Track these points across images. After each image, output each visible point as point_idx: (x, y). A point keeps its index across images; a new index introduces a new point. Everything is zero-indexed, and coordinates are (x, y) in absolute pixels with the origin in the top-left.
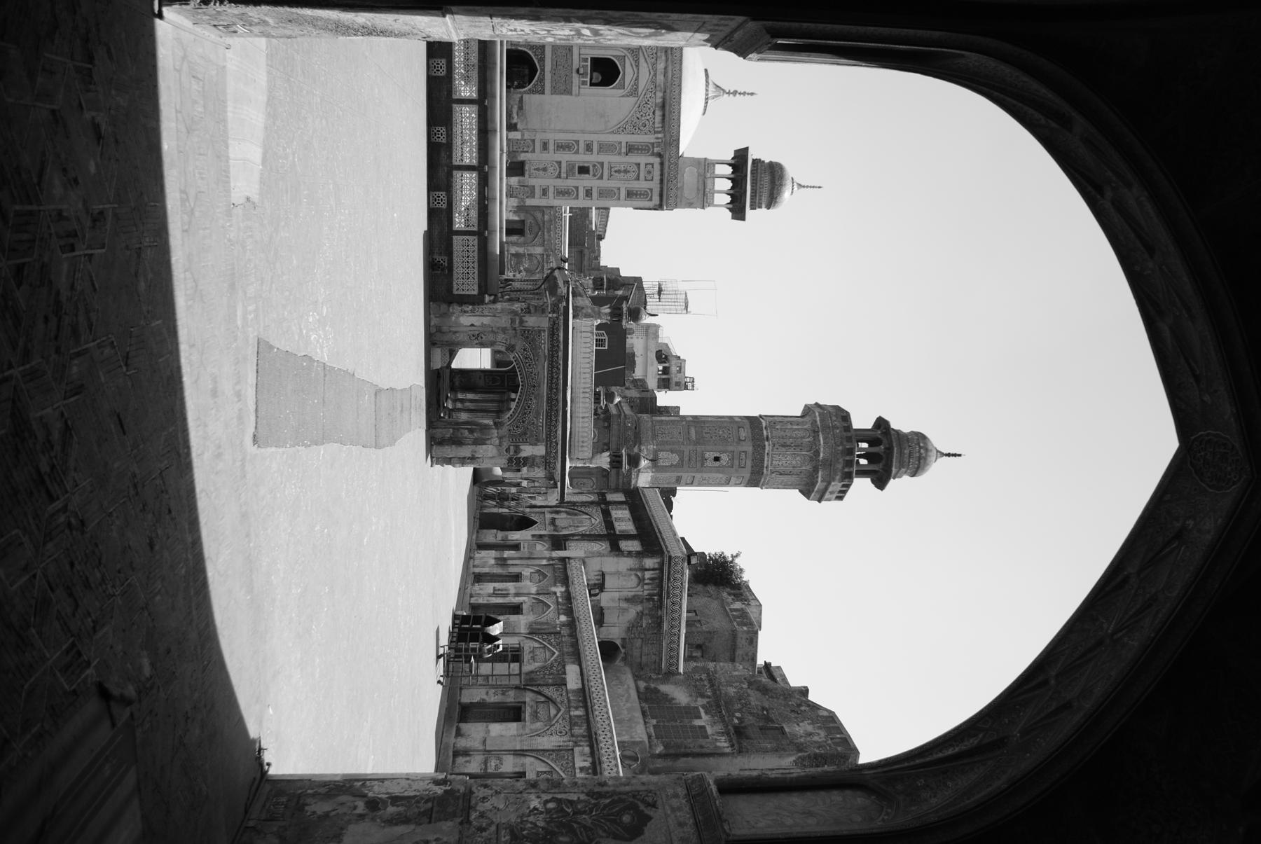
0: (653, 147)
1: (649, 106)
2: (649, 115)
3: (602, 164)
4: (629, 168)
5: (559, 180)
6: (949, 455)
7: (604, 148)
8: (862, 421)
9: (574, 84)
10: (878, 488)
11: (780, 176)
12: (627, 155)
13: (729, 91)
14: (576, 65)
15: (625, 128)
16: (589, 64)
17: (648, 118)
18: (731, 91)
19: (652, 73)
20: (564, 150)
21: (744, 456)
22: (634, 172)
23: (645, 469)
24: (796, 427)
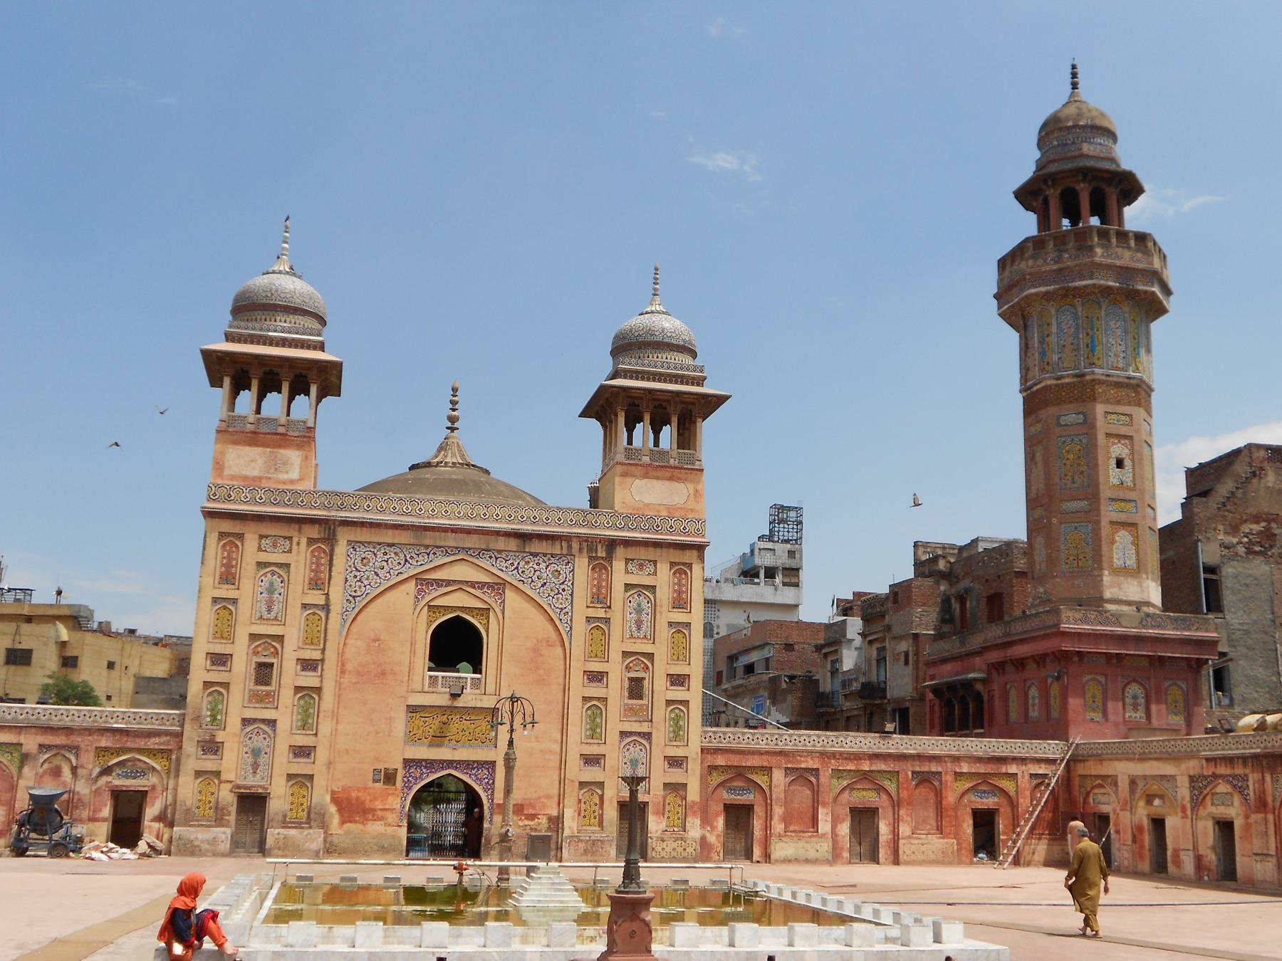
0: (597, 558)
1: (522, 563)
4: (634, 604)
8: (1026, 224)
9: (479, 705)
10: (1135, 199)
12: (610, 607)
13: (448, 428)
14: (442, 700)
17: (543, 565)
18: (449, 425)
23: (1143, 590)
24: (1054, 329)
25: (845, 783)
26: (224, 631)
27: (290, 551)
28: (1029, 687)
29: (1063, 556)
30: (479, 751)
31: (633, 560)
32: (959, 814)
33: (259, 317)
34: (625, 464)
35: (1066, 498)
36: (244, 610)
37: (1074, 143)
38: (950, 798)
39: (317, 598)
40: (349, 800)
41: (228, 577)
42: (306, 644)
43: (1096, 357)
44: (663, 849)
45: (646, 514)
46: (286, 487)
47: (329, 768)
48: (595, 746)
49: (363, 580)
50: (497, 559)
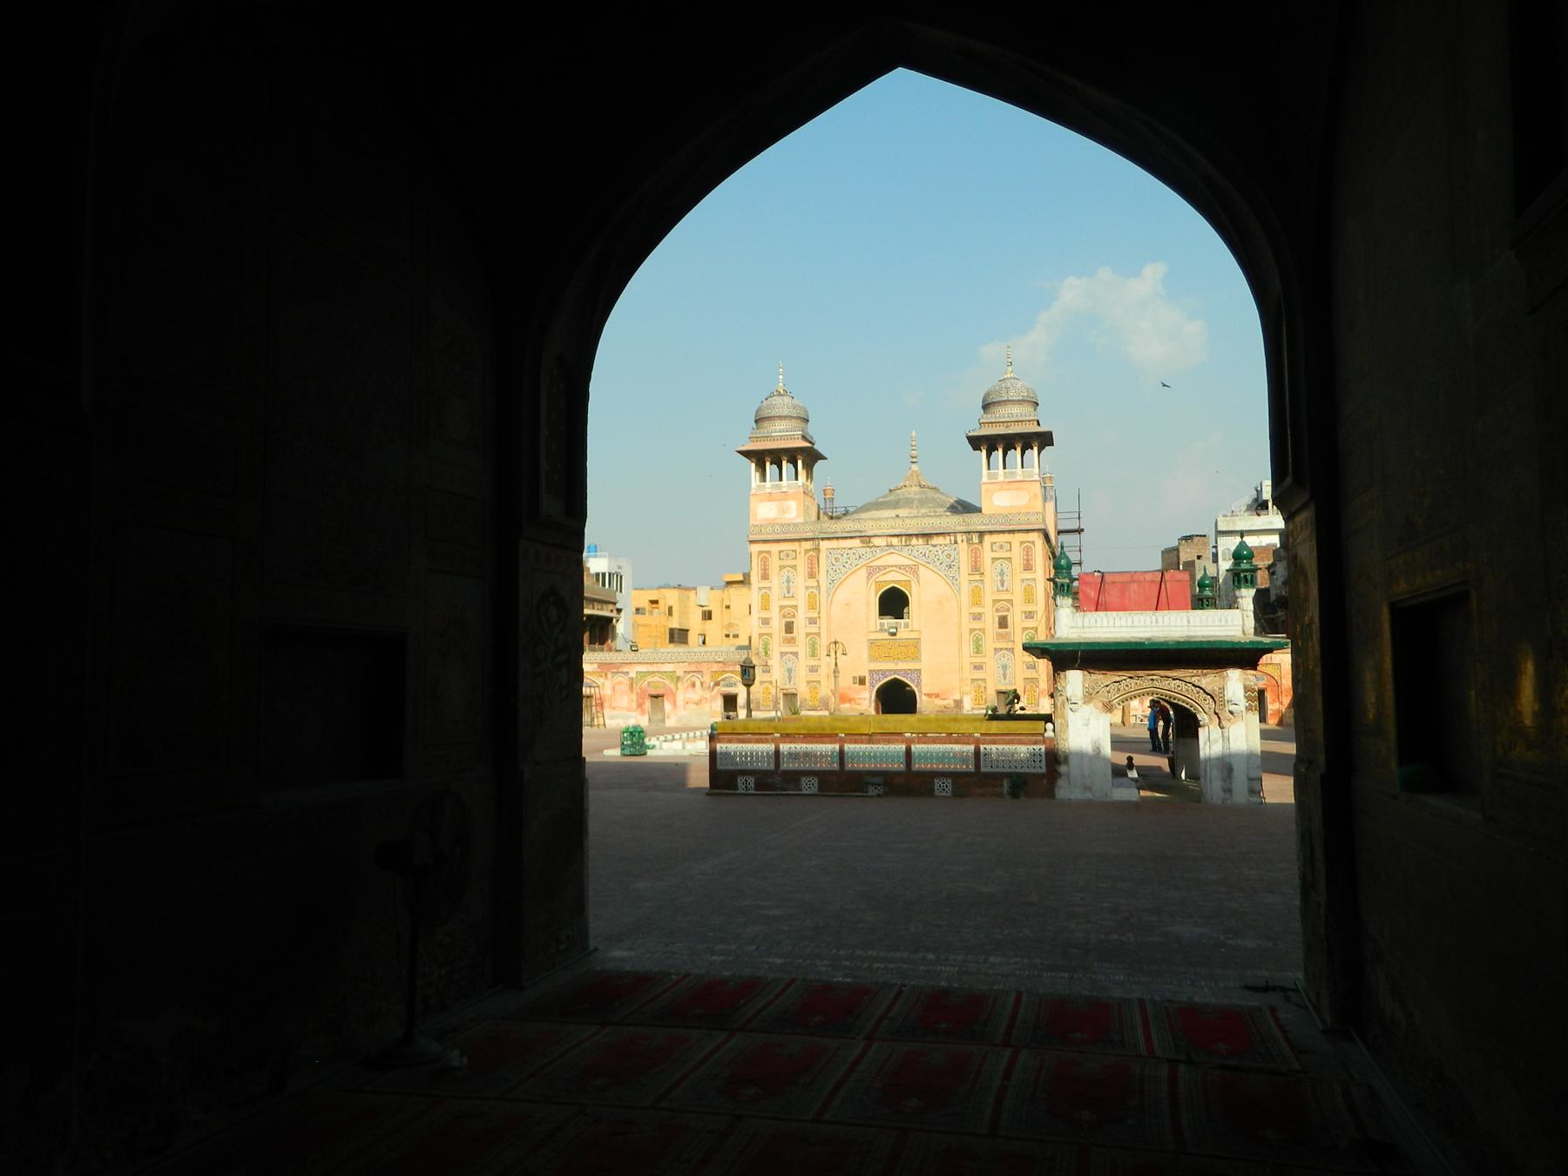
0: (973, 544)
1: (927, 552)
3: (995, 601)
5: (1015, 650)
7: (977, 599)
17: (940, 552)
20: (981, 645)
26: (765, 606)
27: (796, 558)
39: (813, 583)
41: (765, 577)
46: (790, 522)
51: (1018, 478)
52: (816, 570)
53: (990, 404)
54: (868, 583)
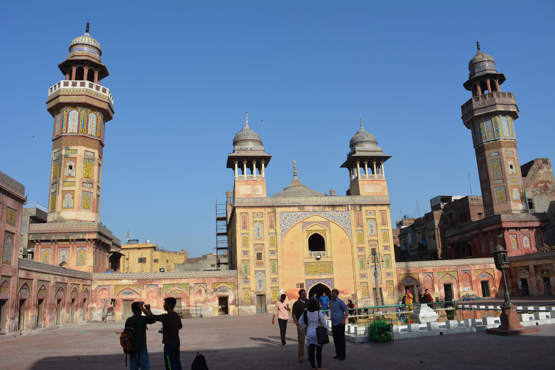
1: (334, 215)
2: (339, 214)
4: (370, 225)
6: (479, 49)
11: (362, 138)
15: (348, 228)
16: (313, 252)
17: (340, 215)
19: (315, 214)
21: (508, 152)
22: (371, 222)
25: (441, 276)
26: (245, 244)
27: (262, 217)
28: (489, 241)
29: (496, 198)
30: (328, 275)
31: (367, 211)
32: (477, 283)
33: (243, 144)
34: (361, 181)
35: (495, 180)
36: (251, 236)
37: (482, 66)
38: (474, 278)
40: (290, 294)
41: (245, 227)
42: (271, 246)
43: (500, 134)
44: (388, 302)
45: (370, 195)
46: (258, 197)
47: (283, 284)
48: (364, 271)
49: (286, 224)
50: (326, 214)
51: (376, 179)
52: (274, 224)
53: (359, 142)
54: (303, 232)
